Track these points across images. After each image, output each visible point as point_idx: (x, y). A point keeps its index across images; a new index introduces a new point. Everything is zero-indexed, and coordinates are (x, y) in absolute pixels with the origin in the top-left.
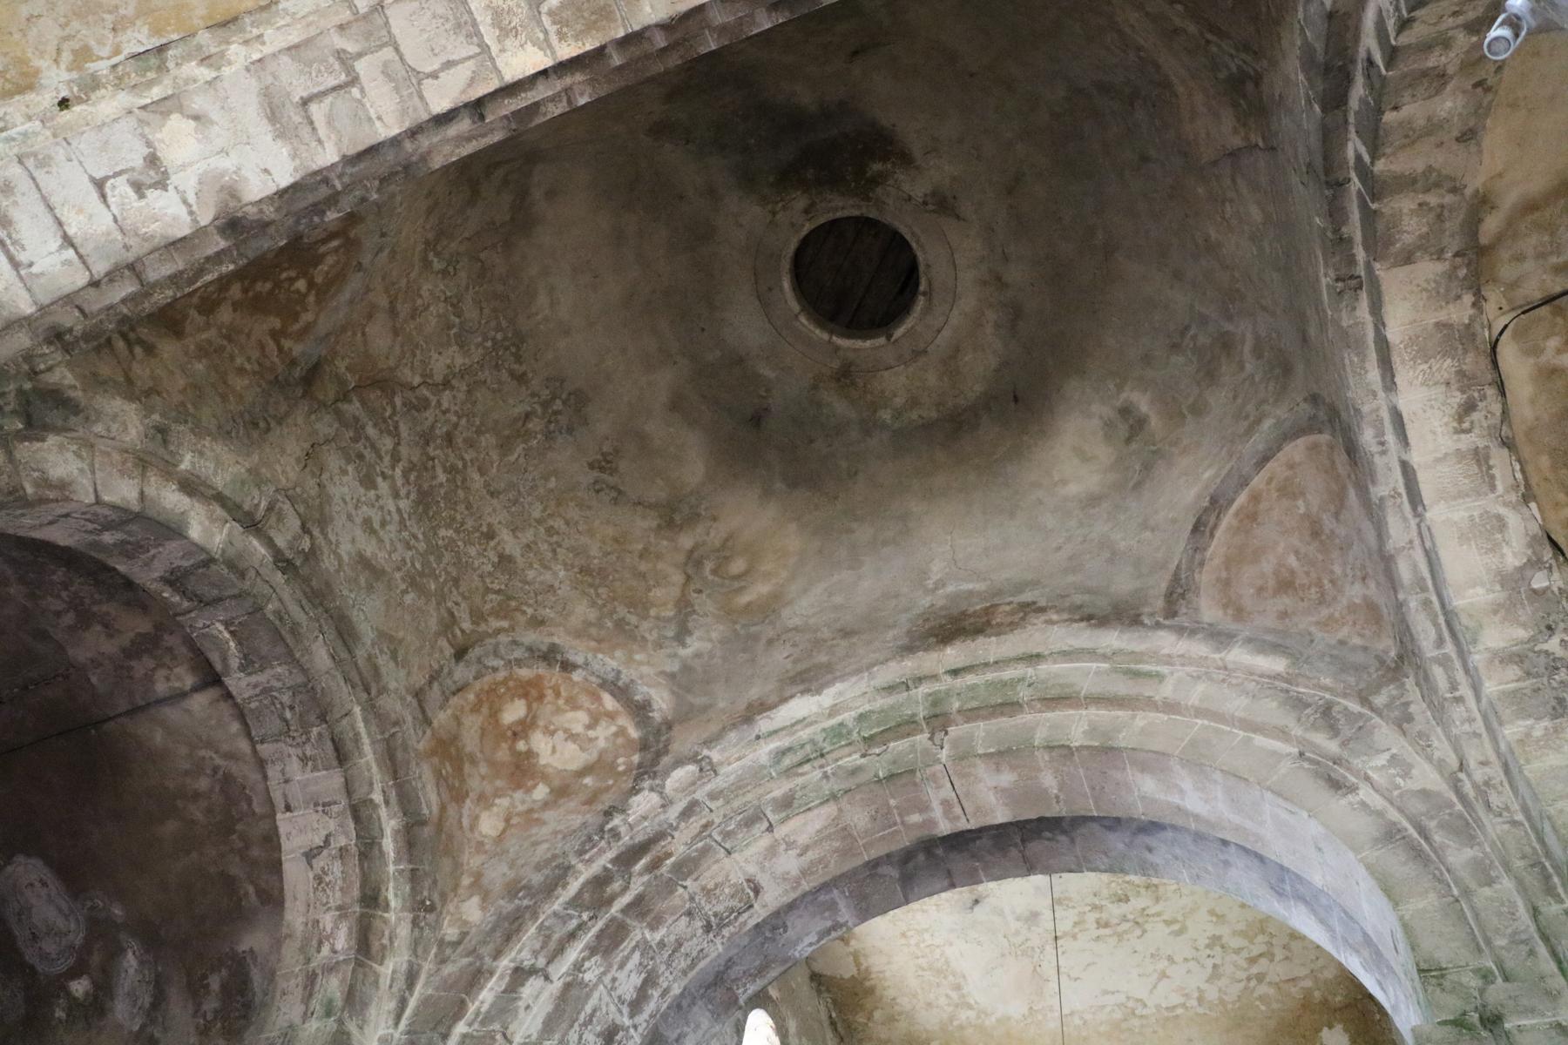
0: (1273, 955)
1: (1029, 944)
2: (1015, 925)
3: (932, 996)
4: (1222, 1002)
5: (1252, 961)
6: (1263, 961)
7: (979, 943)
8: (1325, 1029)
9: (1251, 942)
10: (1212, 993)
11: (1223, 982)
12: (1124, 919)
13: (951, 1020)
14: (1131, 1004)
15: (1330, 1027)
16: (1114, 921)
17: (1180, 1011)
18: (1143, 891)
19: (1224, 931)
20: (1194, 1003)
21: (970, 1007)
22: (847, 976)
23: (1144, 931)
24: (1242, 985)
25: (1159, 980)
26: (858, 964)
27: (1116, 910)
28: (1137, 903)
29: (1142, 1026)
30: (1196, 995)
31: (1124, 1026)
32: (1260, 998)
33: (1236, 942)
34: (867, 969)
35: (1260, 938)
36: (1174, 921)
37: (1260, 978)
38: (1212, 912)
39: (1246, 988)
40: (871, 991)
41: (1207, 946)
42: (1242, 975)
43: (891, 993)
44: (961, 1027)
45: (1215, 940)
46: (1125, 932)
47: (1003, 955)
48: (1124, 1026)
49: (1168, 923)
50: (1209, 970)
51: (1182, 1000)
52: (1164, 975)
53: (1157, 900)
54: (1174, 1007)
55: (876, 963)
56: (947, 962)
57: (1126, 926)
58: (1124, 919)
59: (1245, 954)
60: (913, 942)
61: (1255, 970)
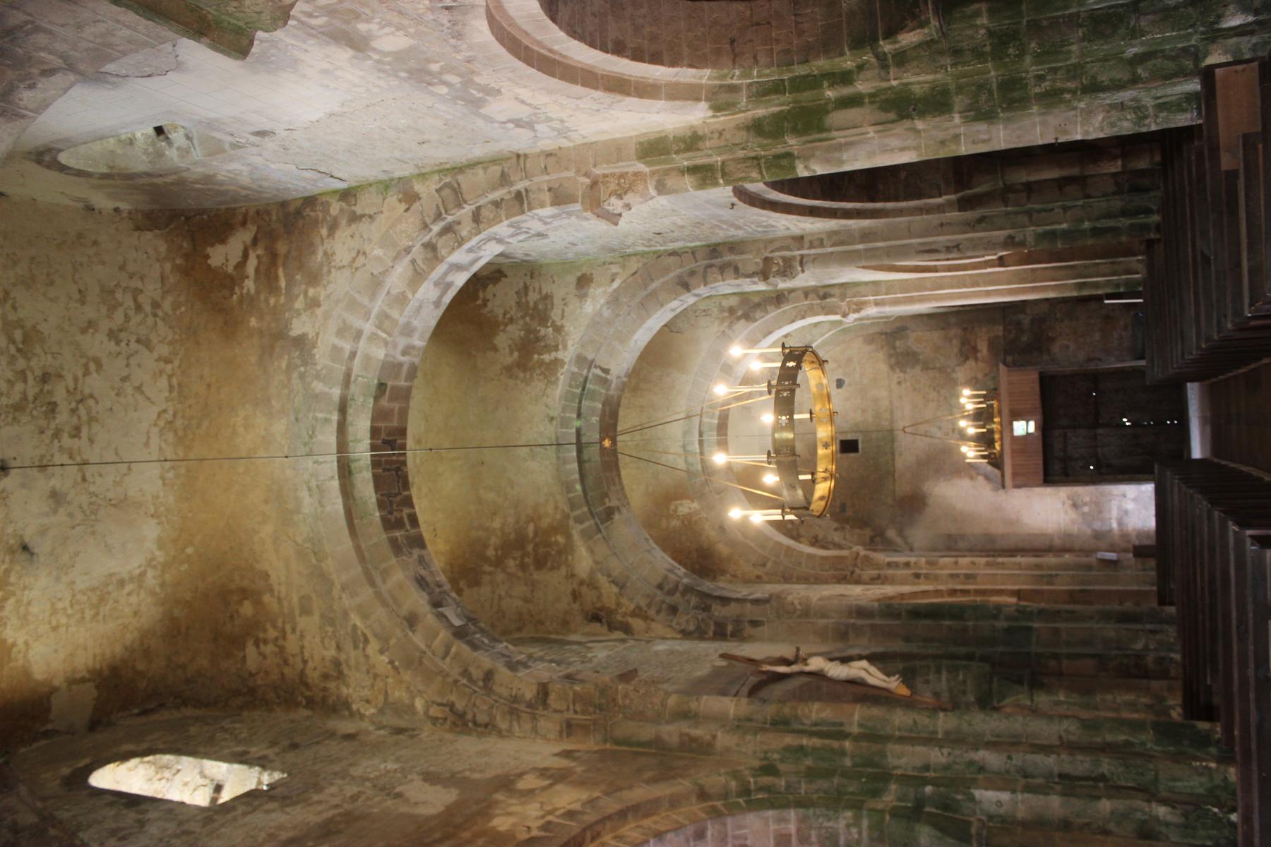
0: (136, 289)
1: (85, 507)
2: (62, 516)
3: (127, 610)
4: (171, 343)
5: (139, 308)
6: (141, 299)
7: (77, 554)
8: (209, 262)
9: (121, 305)
10: (164, 350)
11: (154, 339)
12: (74, 411)
13: (153, 593)
14: (162, 423)
15: (208, 257)
16: (75, 420)
17: (174, 381)
18: (47, 387)
19: (105, 325)
20: (169, 367)
21: (142, 574)
22: (95, 693)
23: (91, 396)
24: (160, 323)
25: (142, 393)
26: (83, 680)
27: (63, 416)
28: (60, 394)
29: (183, 417)
30: (162, 364)
31: (181, 433)
32: (174, 309)
33: (119, 316)
34: (89, 671)
35: (119, 295)
36: (86, 366)
37: (156, 305)
38: (84, 331)
39: (163, 319)
40: (115, 670)
41: (118, 343)
42: (150, 320)
43: (118, 649)
44: (163, 585)
45: (113, 335)
46: (89, 413)
47: (93, 533)
48: (181, 433)
49: (87, 373)
50: (141, 347)
51: (165, 378)
52: (139, 389)
53: (60, 376)
54: (171, 386)
55: (83, 662)
56: (93, 589)
57: (82, 411)
58: (74, 411)
59: (131, 313)
60: (64, 620)
61: (148, 308)
